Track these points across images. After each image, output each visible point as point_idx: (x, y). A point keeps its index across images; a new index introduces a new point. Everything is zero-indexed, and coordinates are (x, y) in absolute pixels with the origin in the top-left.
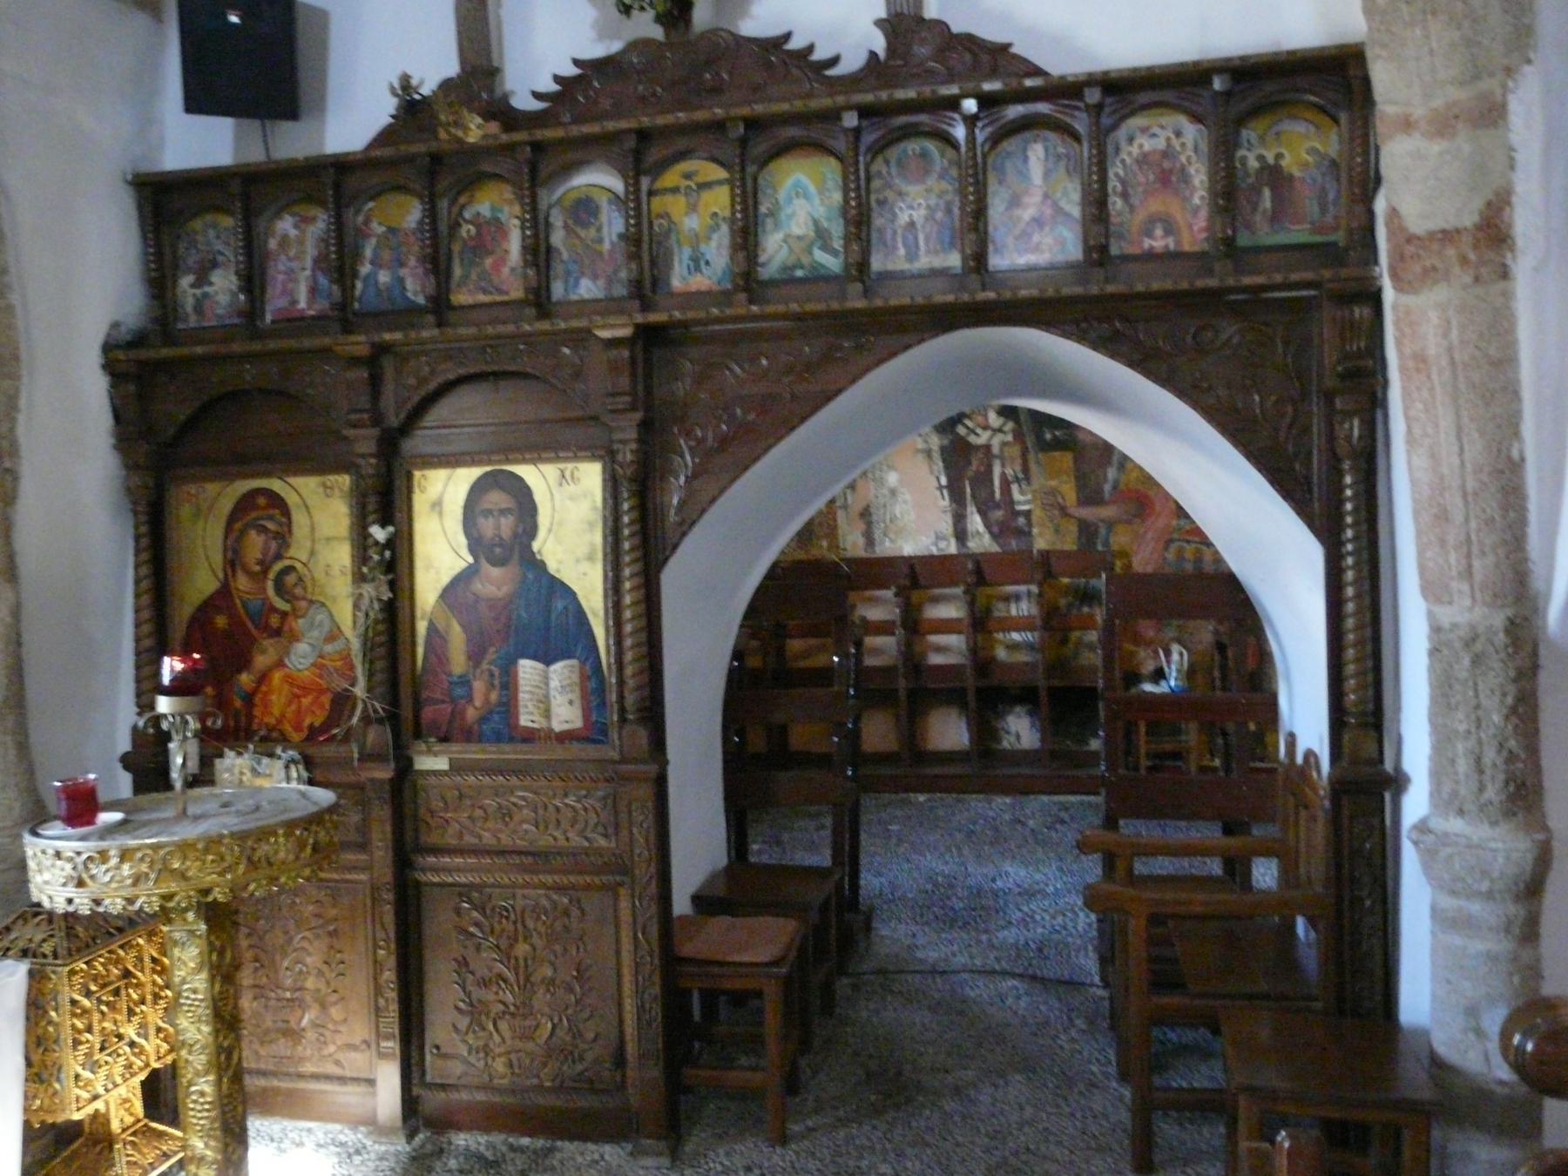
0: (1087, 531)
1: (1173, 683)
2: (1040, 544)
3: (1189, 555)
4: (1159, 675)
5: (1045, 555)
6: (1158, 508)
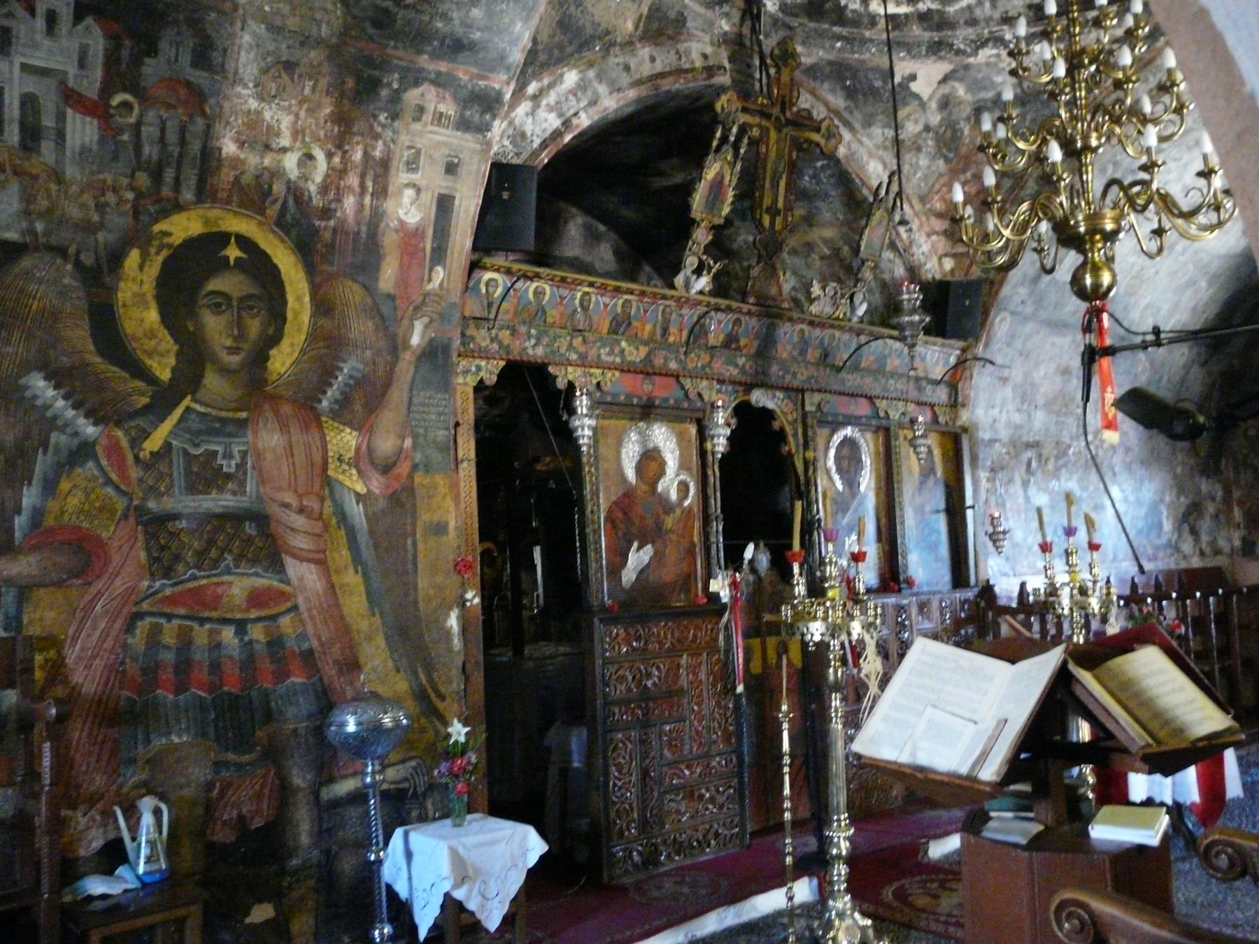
1: (141, 869)
3: (169, 638)
4: (113, 856)
6: (116, 559)
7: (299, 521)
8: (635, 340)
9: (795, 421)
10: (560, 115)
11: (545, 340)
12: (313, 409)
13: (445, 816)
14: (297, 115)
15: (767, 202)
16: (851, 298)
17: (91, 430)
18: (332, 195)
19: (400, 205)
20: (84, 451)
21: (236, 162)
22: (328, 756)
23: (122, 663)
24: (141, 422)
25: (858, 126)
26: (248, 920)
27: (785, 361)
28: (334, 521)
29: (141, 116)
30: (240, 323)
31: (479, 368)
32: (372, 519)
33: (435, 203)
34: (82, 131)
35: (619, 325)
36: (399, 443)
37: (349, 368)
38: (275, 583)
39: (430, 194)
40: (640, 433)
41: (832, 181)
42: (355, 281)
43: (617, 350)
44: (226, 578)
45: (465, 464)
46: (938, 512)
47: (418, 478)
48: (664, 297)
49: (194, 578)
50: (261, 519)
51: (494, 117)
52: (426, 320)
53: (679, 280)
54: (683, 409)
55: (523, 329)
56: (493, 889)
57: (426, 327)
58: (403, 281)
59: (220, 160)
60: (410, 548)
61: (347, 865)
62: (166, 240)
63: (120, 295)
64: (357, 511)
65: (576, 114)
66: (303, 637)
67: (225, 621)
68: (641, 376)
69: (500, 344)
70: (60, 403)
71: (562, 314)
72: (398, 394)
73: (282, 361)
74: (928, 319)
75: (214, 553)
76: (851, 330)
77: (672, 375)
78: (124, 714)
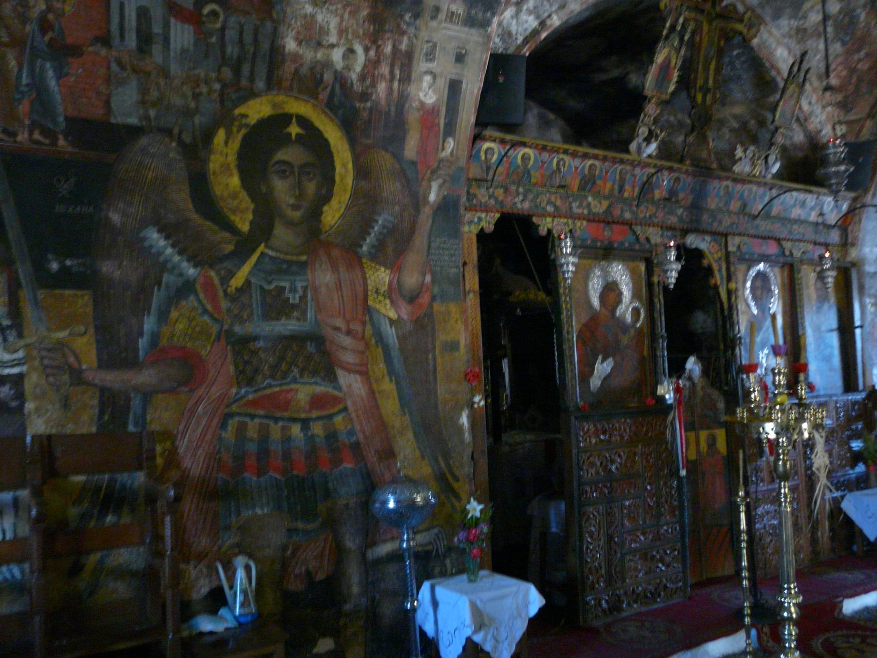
0: (113, 404)
2: (38, 425)
3: (252, 431)
4: (217, 600)
5: (46, 443)
7: (347, 341)
8: (598, 195)
9: (720, 259)
10: (537, 17)
11: (531, 196)
12: (356, 253)
13: (461, 572)
14: (342, 17)
15: (700, 82)
16: (766, 158)
17: (191, 271)
18: (368, 82)
19: (420, 89)
20: (186, 288)
21: (296, 57)
22: (372, 525)
23: (219, 452)
24: (228, 264)
25: (768, 19)
26: (315, 651)
27: (712, 211)
28: (373, 341)
29: (225, 21)
30: (300, 185)
31: (480, 219)
32: (402, 339)
33: (447, 86)
34: (182, 35)
35: (586, 184)
36: (420, 279)
37: (382, 220)
38: (330, 390)
39: (443, 80)
40: (602, 270)
41: (745, 66)
42: (387, 150)
43: (584, 204)
44: (293, 386)
45: (471, 295)
46: (832, 330)
47: (437, 307)
48: (622, 162)
49: (270, 386)
50: (319, 340)
51: (493, 14)
52: (440, 181)
53: (633, 147)
55: (514, 188)
56: (503, 634)
57: (440, 187)
58: (423, 150)
59: (283, 54)
60: (431, 362)
61: (387, 610)
62: (244, 121)
63: (211, 165)
64: (390, 333)
65: (549, 16)
66: (351, 433)
67: (294, 420)
68: (602, 225)
69: (496, 199)
70: (169, 251)
71: (542, 176)
72: (420, 240)
73: (332, 215)
74: (852, 170)
75: (284, 366)
76: (765, 184)
77: (627, 224)
78: (221, 492)
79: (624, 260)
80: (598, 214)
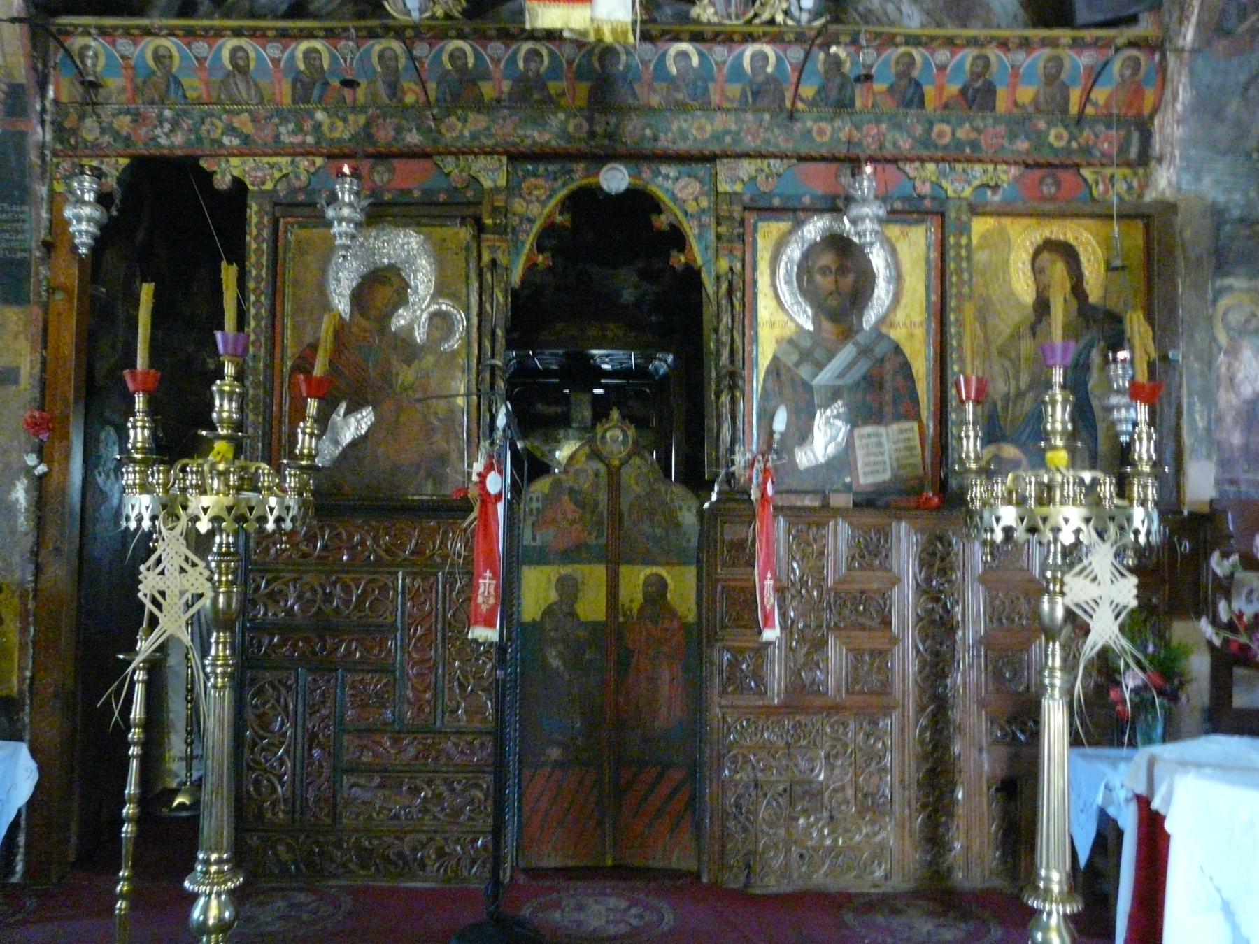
11: (186, 124)
43: (308, 126)
54: (437, 204)
55: (153, 112)
69: (116, 135)
79: (419, 224)
80: (339, 140)
